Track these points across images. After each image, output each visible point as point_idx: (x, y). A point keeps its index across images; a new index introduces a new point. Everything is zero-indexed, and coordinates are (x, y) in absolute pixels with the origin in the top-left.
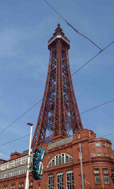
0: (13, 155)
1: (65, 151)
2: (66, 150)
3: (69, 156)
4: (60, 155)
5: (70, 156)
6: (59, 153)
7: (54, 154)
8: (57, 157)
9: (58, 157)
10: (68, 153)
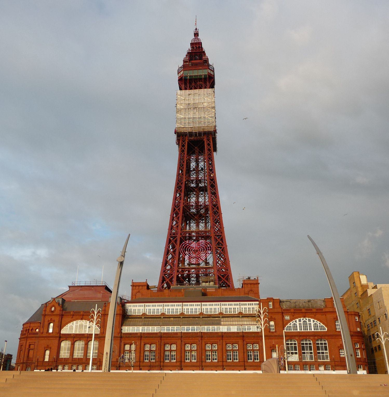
2: (315, 316)
3: (318, 324)
4: (305, 320)
5: (319, 324)
6: (305, 317)
7: (294, 317)
8: (300, 321)
9: (302, 321)
10: (318, 320)
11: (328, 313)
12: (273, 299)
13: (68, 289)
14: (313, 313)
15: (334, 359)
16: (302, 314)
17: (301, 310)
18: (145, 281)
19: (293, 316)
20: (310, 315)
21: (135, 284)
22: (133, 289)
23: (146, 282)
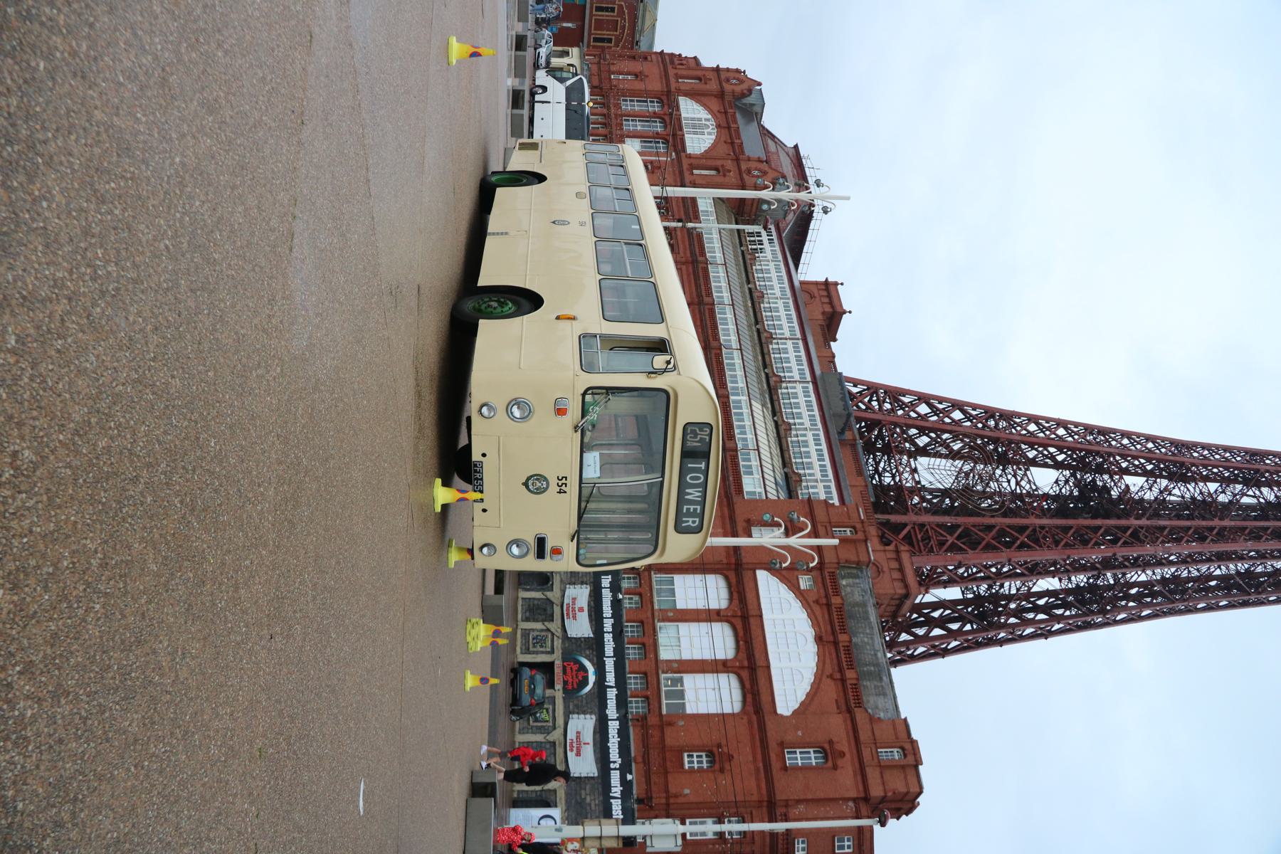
0: (829, 296)
1: (829, 670)
2: (831, 676)
7: (817, 609)
11: (849, 722)
12: (866, 541)
13: (790, 144)
14: (841, 670)
15: (670, 724)
16: (829, 628)
17: (844, 631)
18: (846, 307)
19: (817, 602)
20: (832, 660)
21: (832, 288)
22: (817, 283)
23: (845, 312)
